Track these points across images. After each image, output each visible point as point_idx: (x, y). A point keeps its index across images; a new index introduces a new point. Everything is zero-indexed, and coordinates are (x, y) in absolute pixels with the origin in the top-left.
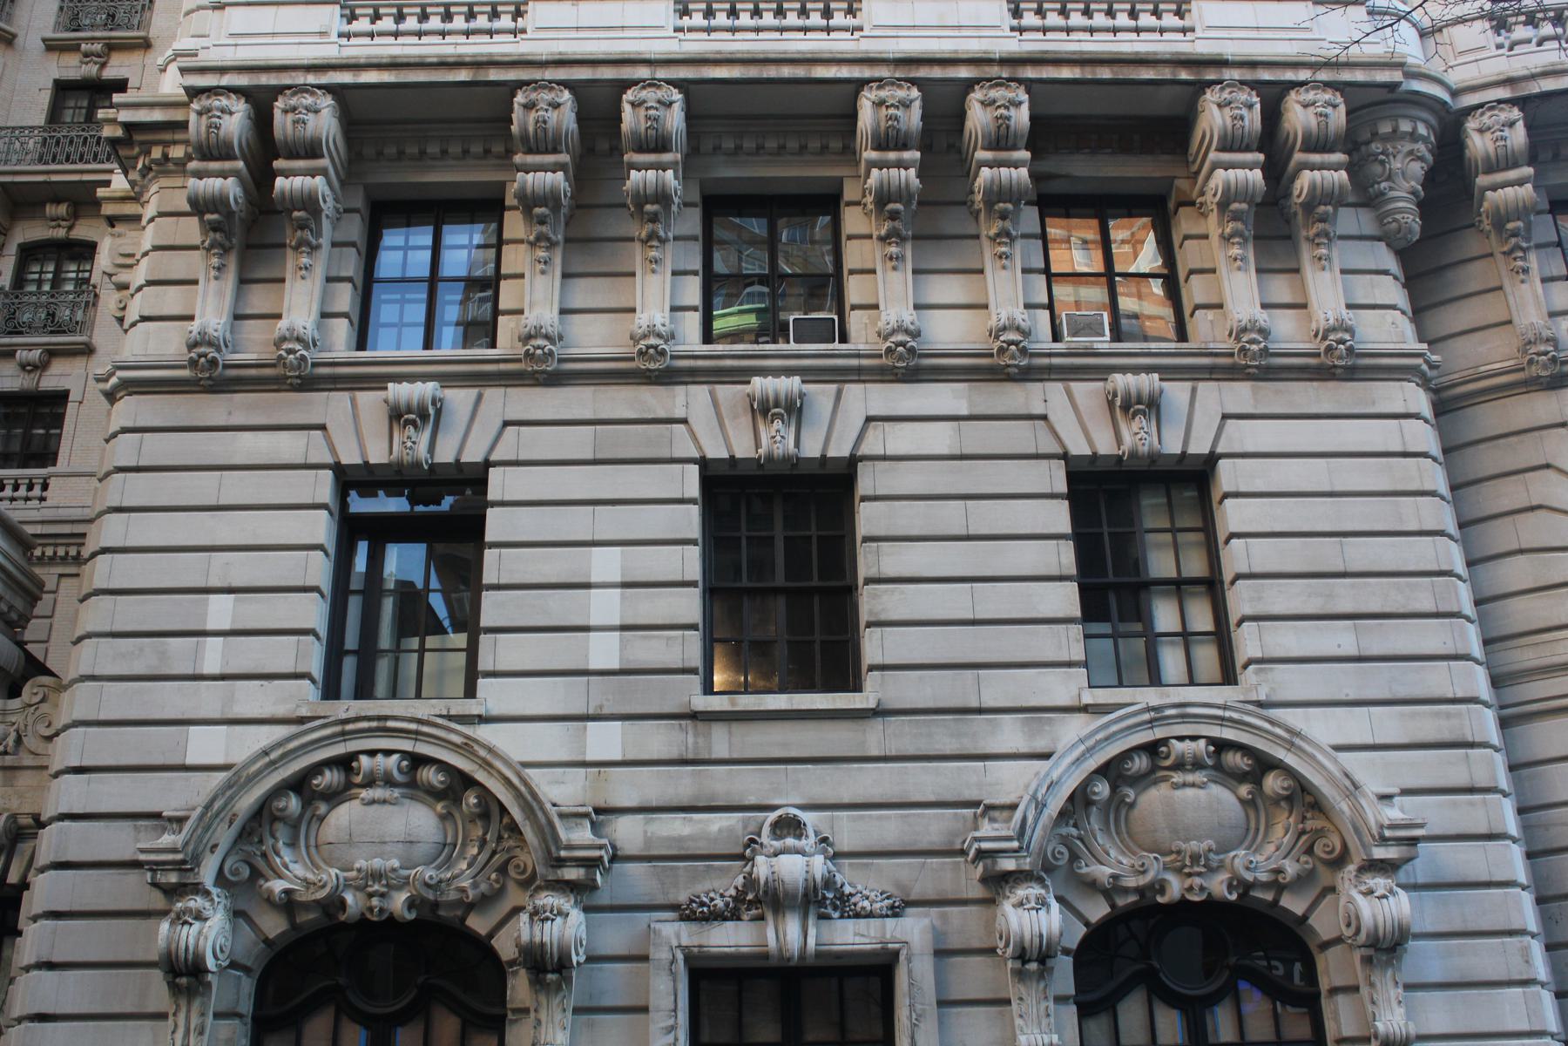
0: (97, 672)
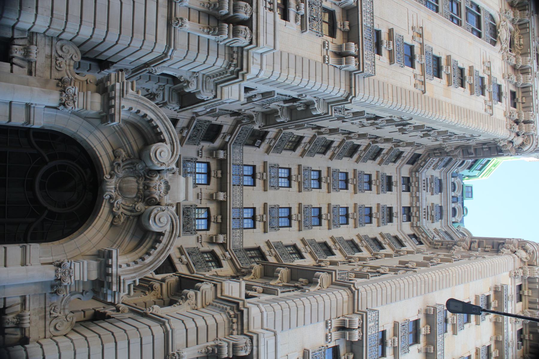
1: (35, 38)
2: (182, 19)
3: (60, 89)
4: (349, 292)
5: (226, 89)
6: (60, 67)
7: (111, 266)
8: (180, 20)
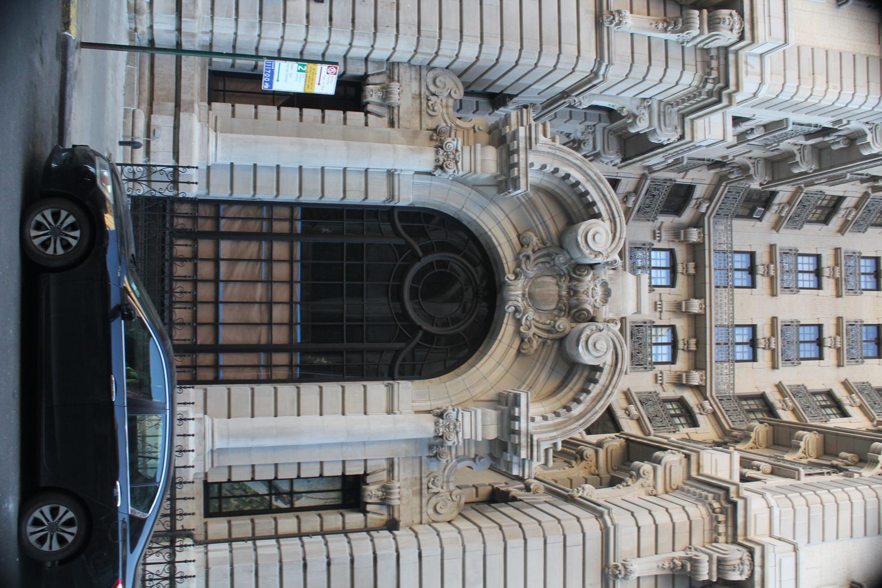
0: (467, 554)
1: (396, 71)
2: (619, 12)
3: (434, 144)
5: (699, 123)
6: (434, 110)
7: (518, 419)
8: (616, 14)
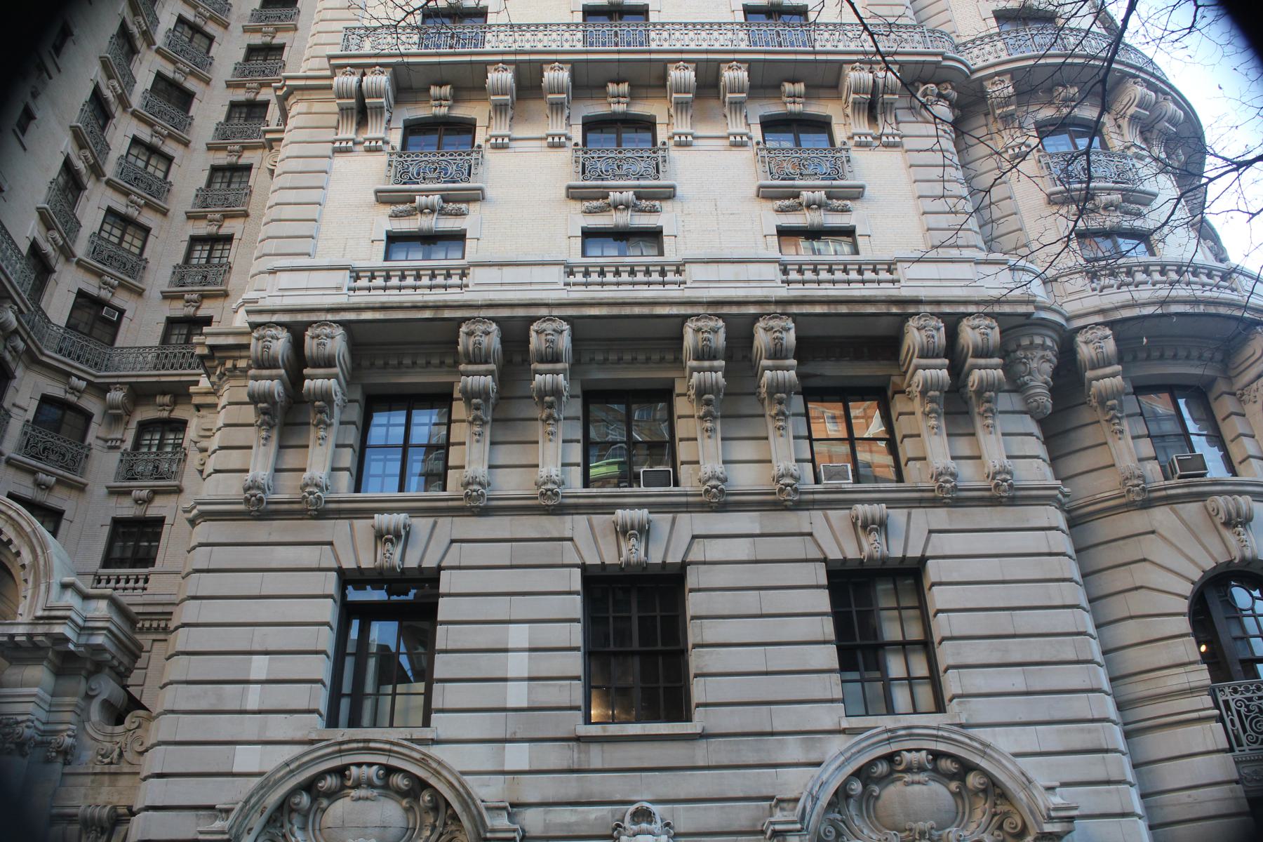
4: (292, 100)
